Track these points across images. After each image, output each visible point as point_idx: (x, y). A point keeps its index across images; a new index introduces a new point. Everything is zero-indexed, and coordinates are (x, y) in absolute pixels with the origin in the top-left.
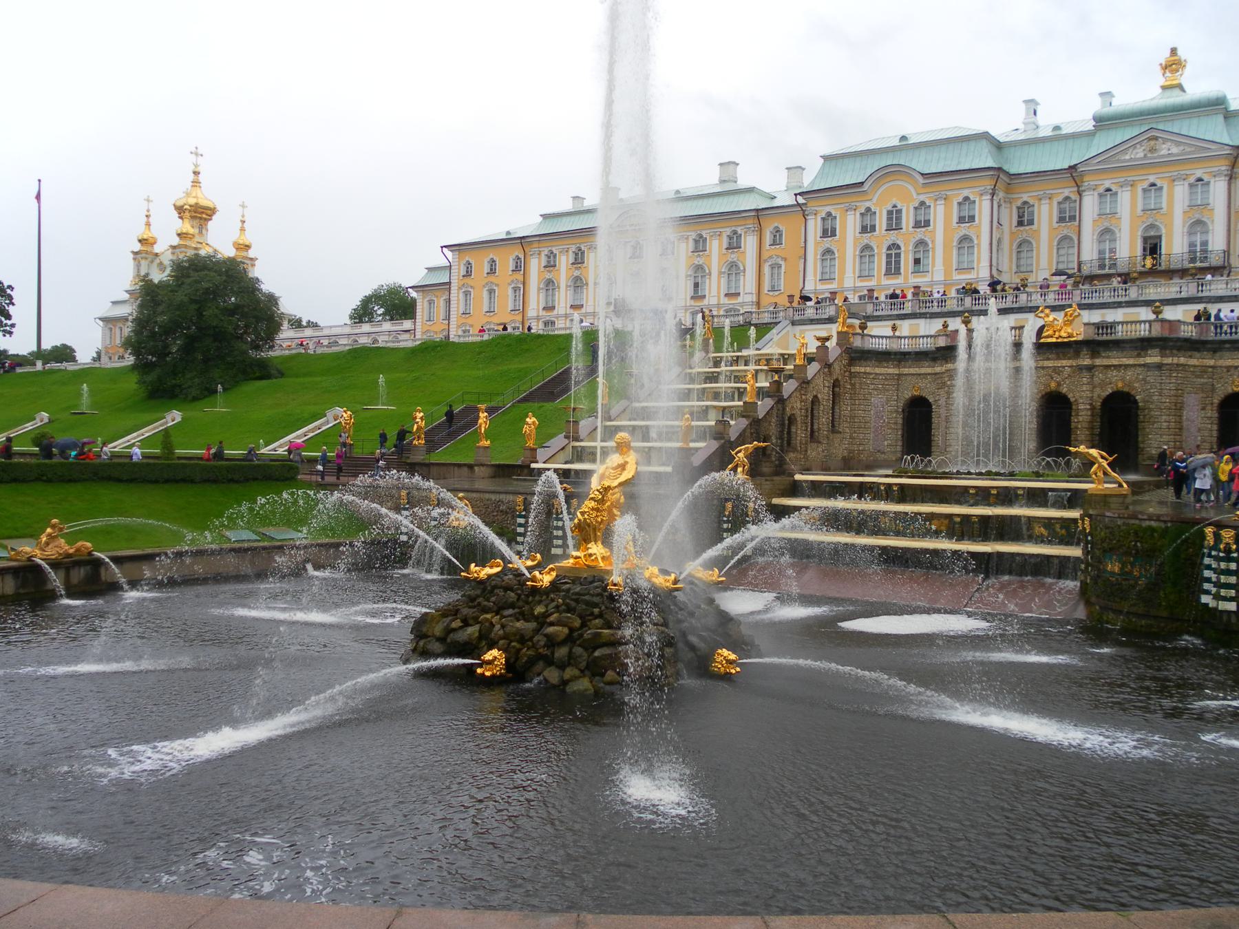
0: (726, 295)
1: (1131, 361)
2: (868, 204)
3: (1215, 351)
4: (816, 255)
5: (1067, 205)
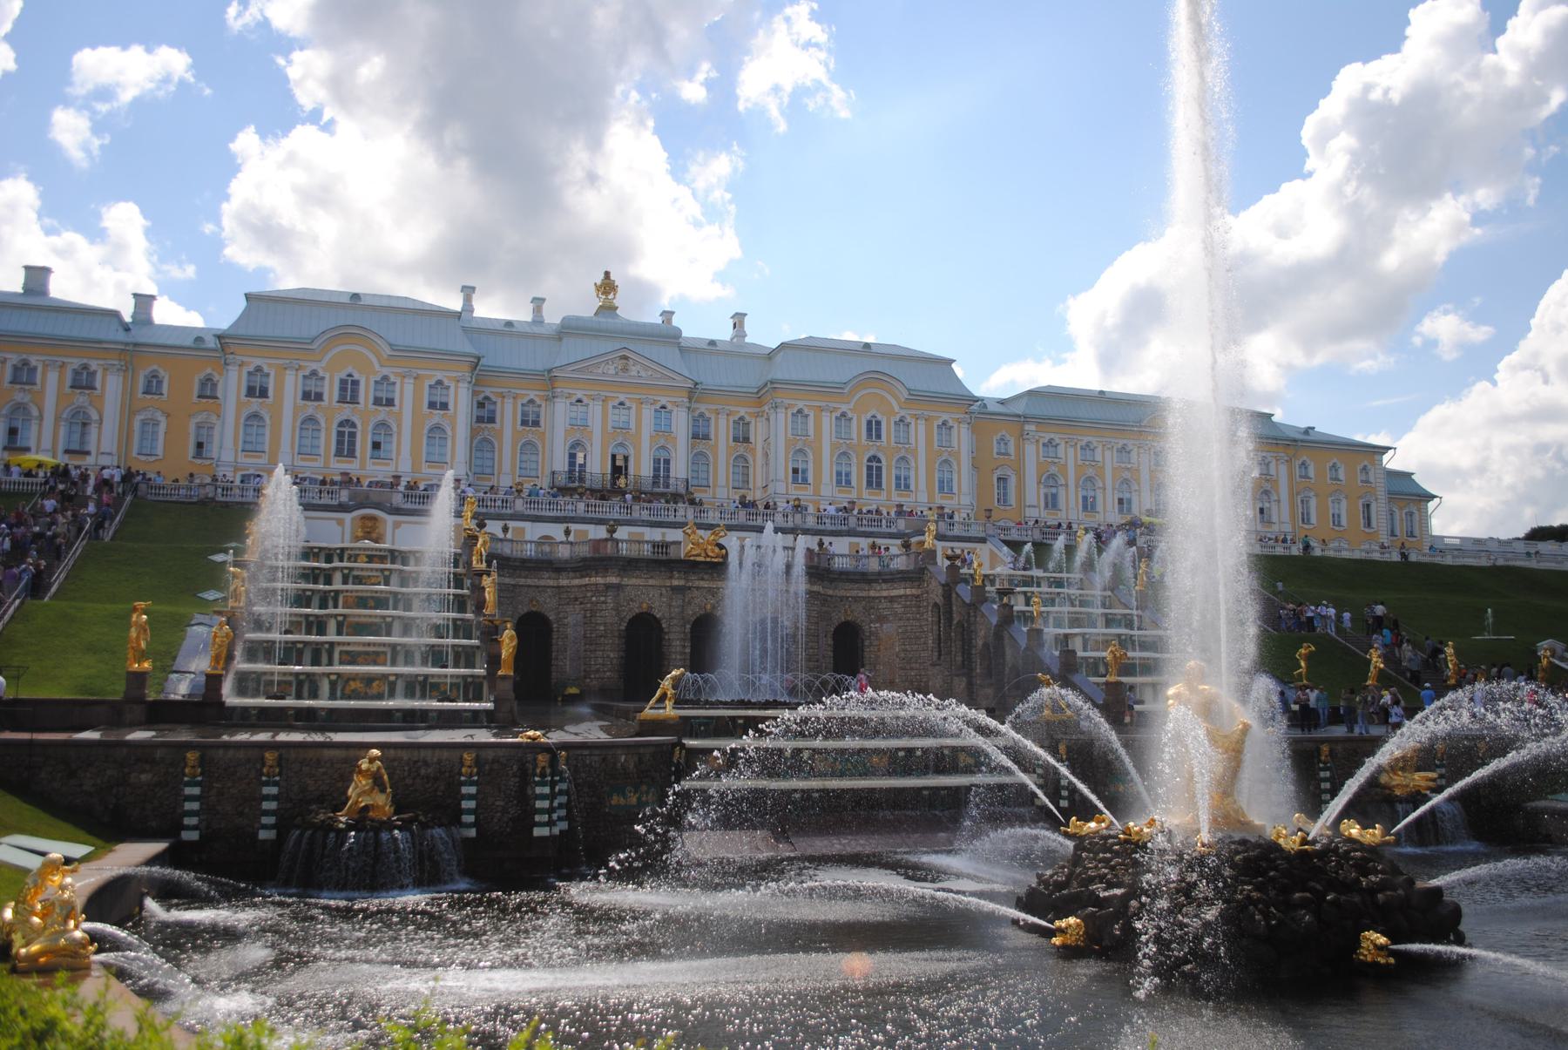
0: (67, 452)
2: (314, 366)
3: (832, 581)
5: (530, 409)
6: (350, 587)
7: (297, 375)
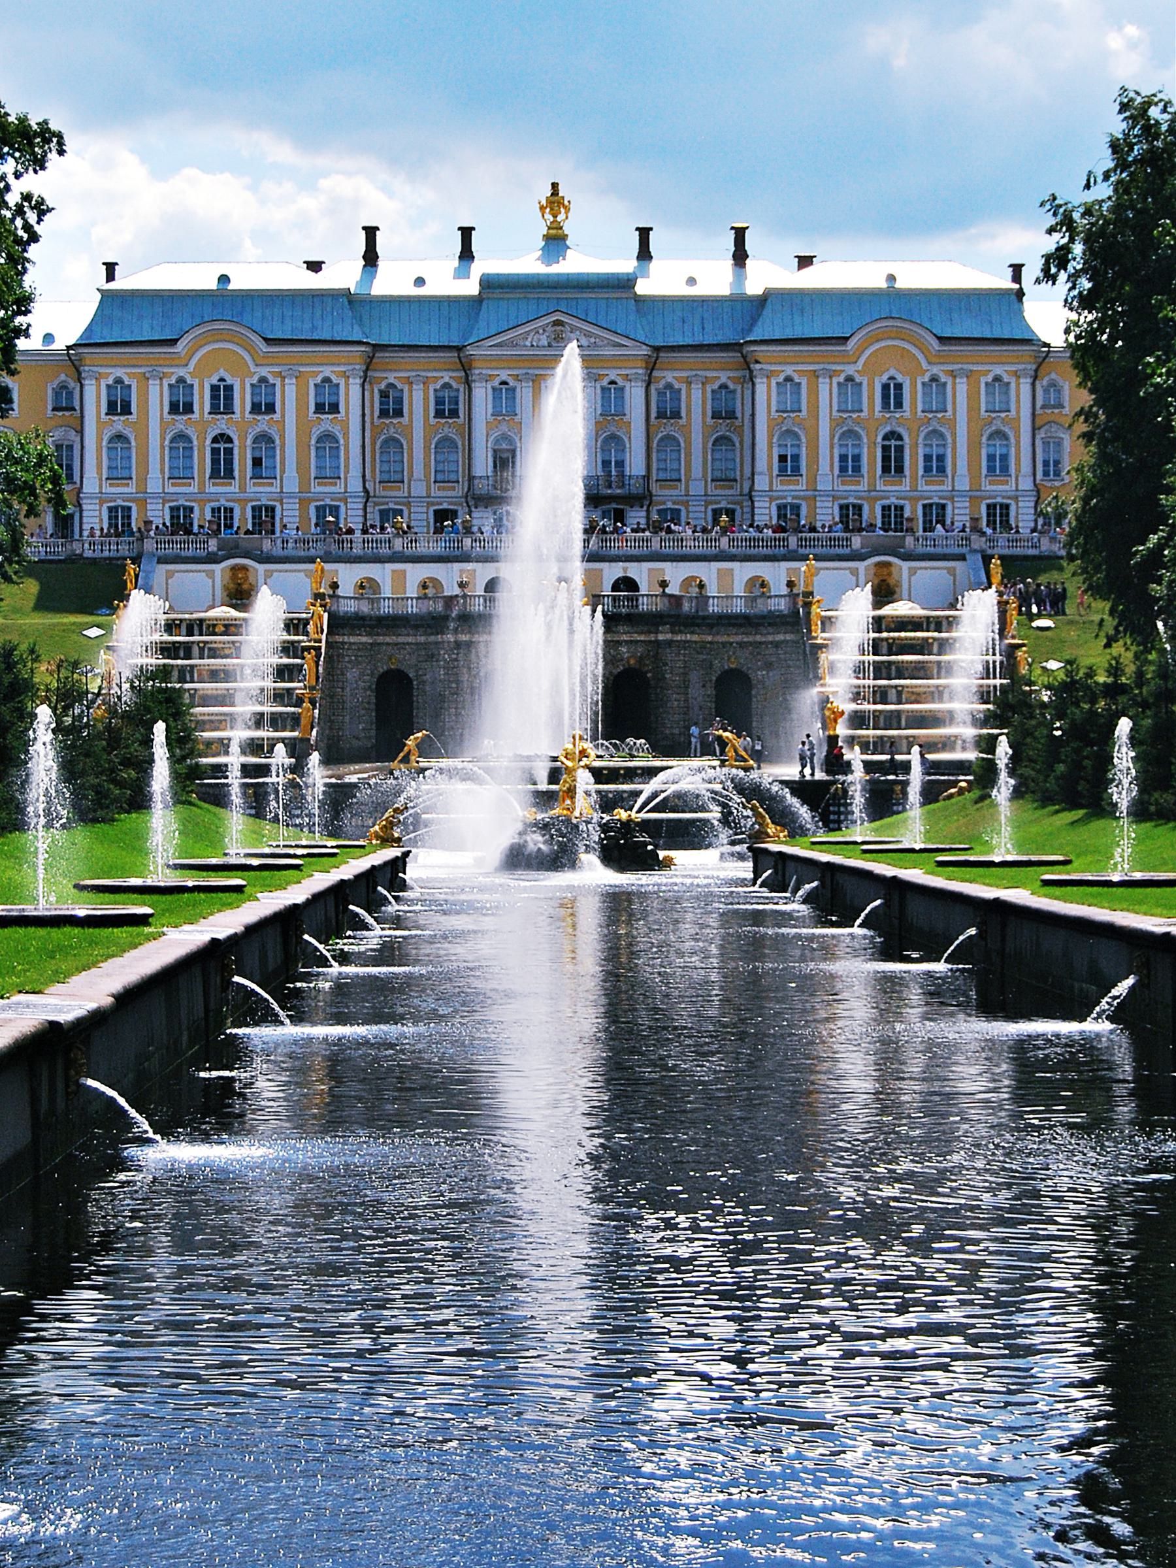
1: (642, 638)
2: (181, 372)
3: (711, 626)
4: (100, 440)
6: (206, 661)
7: (161, 385)
